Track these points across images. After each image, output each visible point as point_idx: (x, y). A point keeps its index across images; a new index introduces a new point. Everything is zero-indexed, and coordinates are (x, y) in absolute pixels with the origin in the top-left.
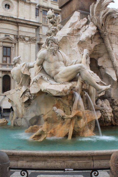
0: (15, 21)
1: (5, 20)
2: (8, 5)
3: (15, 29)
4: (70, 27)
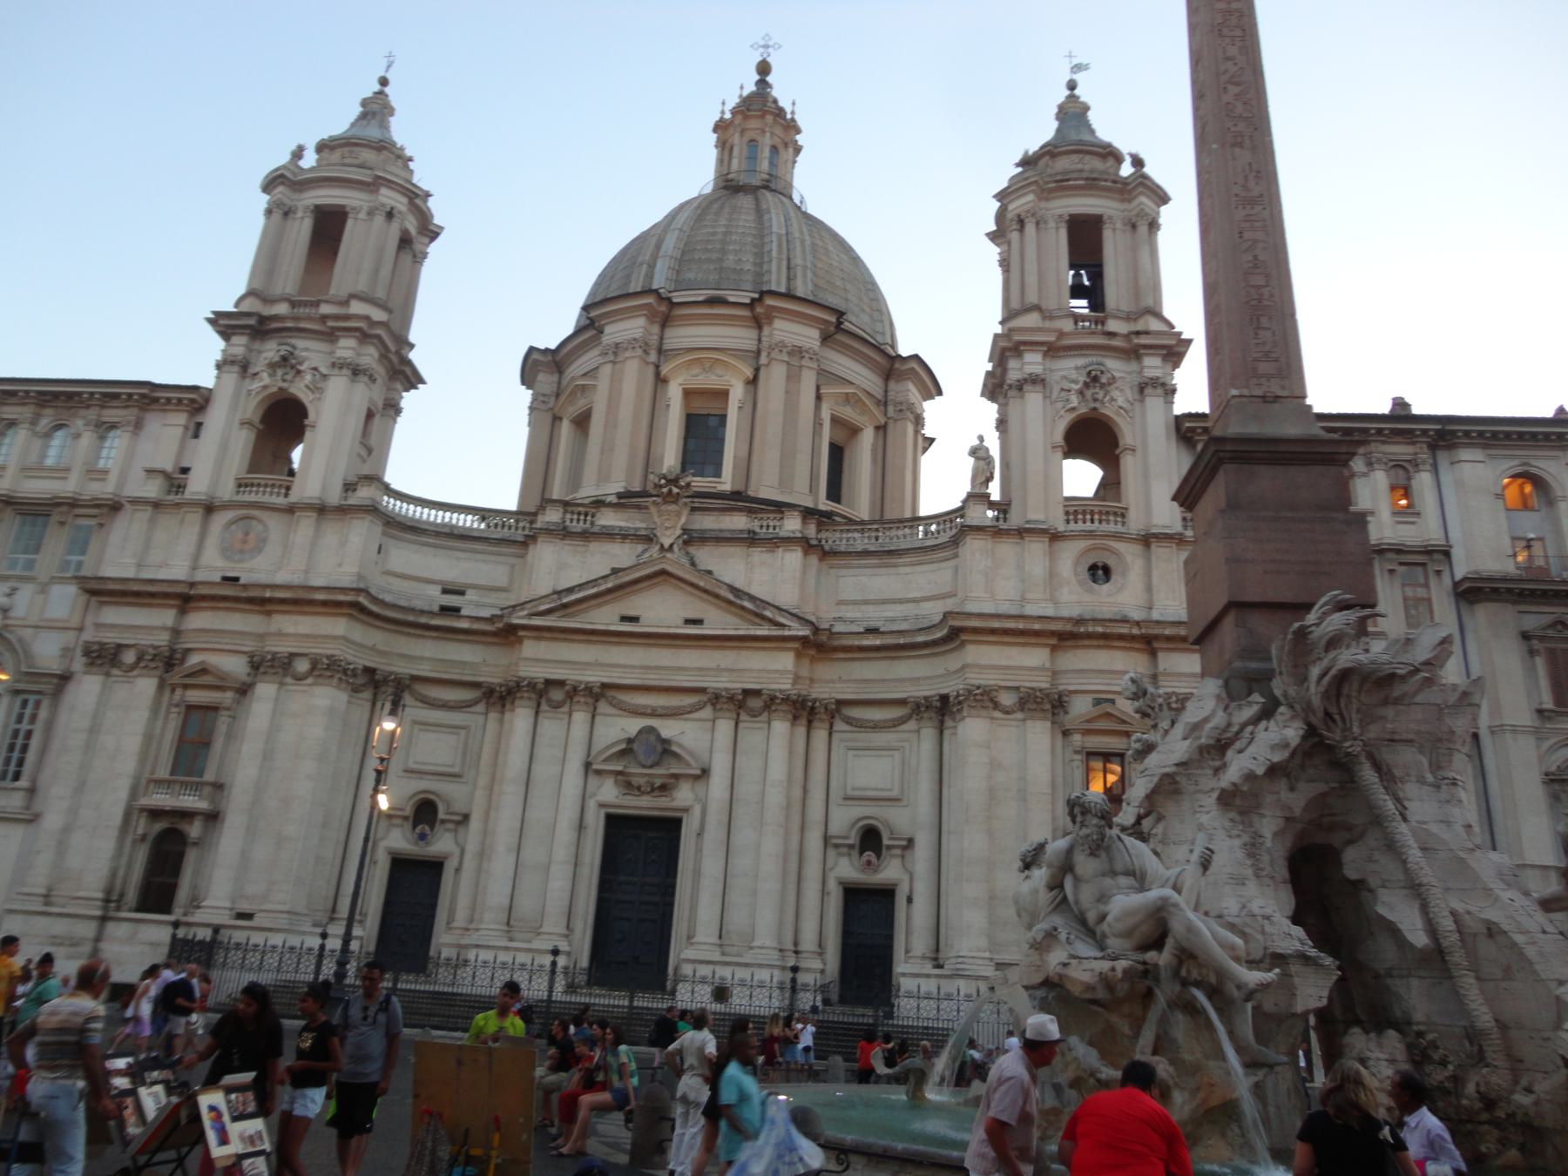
0: (1135, 631)
1: (1090, 636)
2: (1100, 564)
4: (1185, 739)
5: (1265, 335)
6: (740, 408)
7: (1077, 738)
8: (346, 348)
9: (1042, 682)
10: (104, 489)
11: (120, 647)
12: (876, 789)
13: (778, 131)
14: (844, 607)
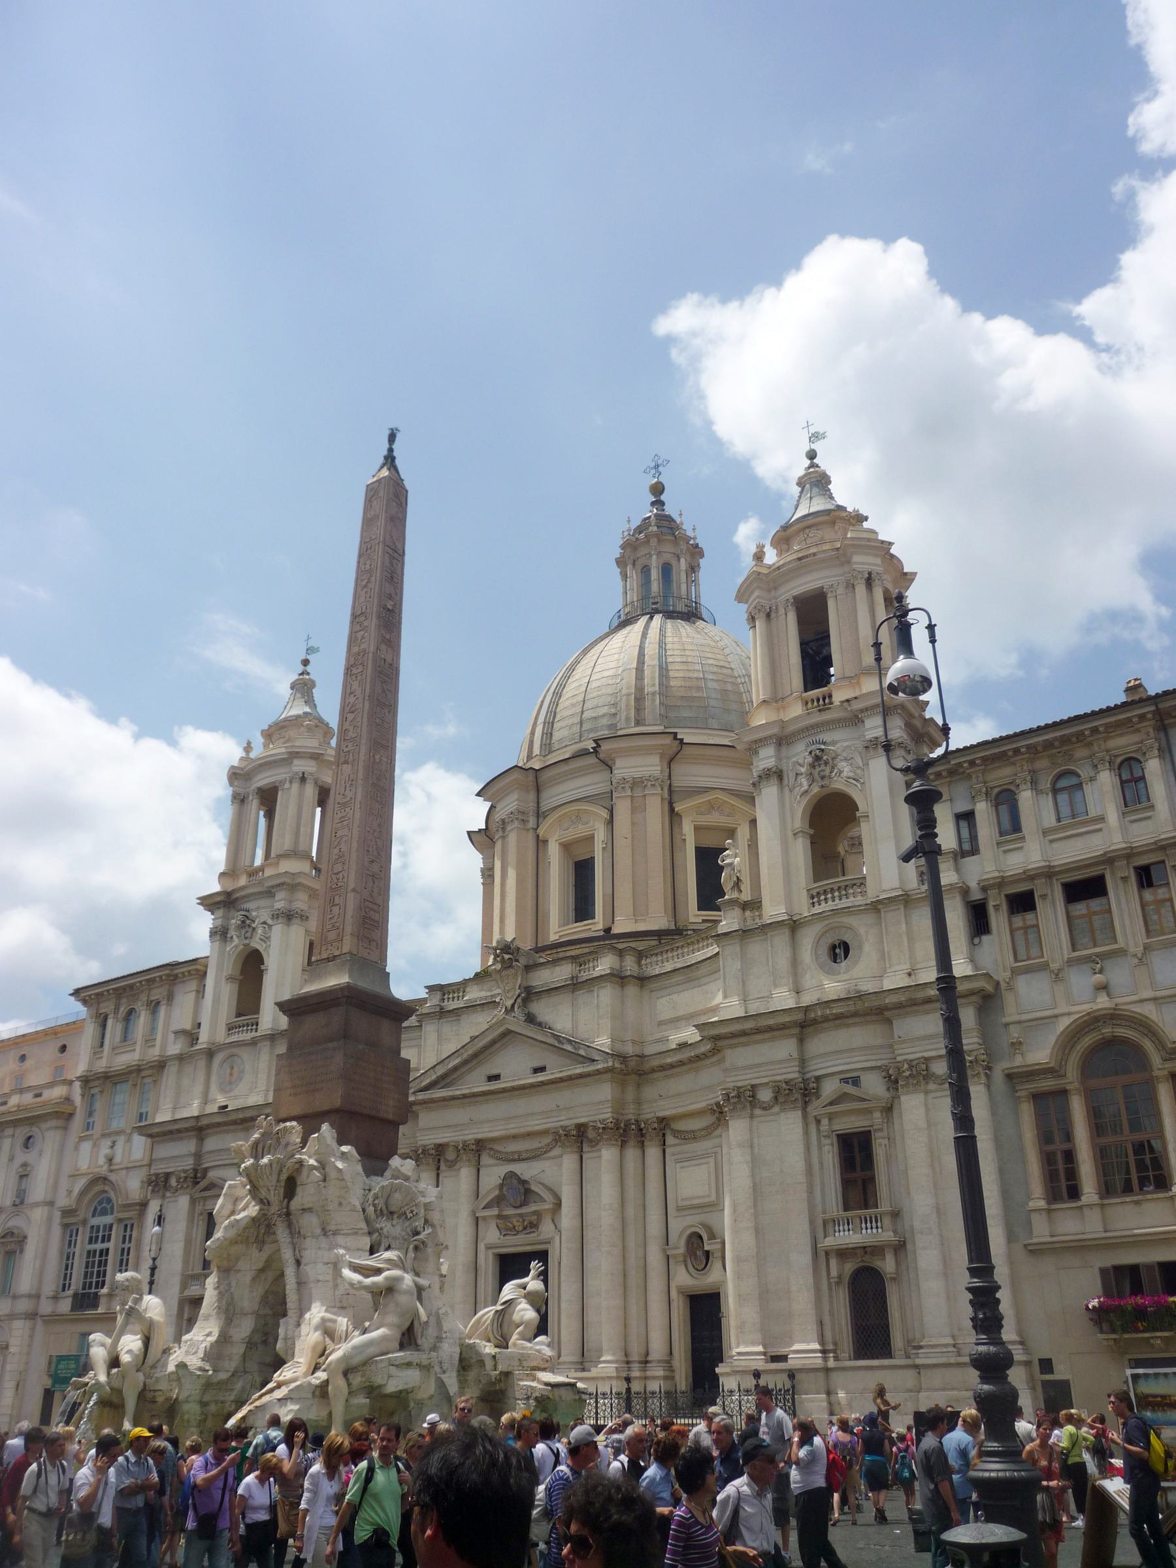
1: (826, 1019)
3: (879, 1042)
5: (336, 910)
6: (603, 848)
7: (825, 1122)
8: (280, 902)
9: (793, 1074)
10: (154, 1053)
11: (167, 1175)
12: (698, 1197)
13: (668, 548)
14: (664, 1027)
